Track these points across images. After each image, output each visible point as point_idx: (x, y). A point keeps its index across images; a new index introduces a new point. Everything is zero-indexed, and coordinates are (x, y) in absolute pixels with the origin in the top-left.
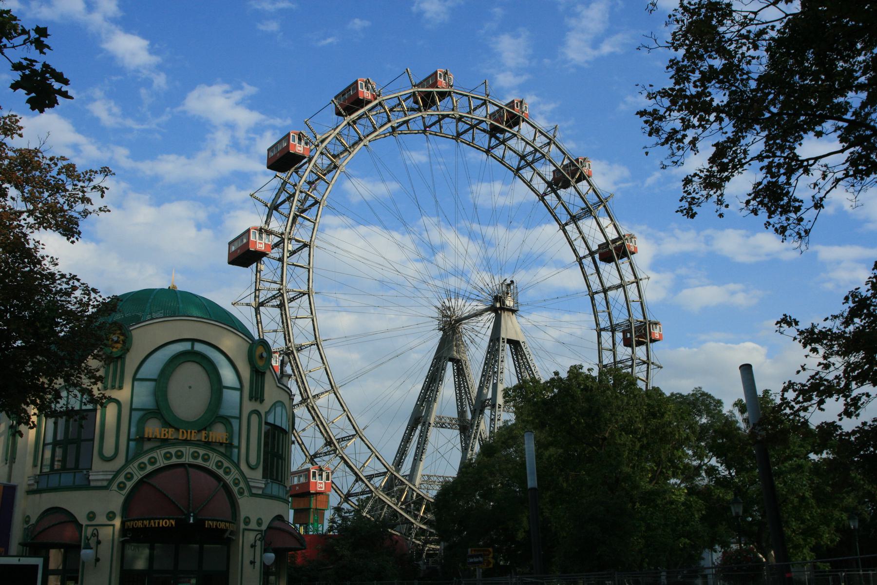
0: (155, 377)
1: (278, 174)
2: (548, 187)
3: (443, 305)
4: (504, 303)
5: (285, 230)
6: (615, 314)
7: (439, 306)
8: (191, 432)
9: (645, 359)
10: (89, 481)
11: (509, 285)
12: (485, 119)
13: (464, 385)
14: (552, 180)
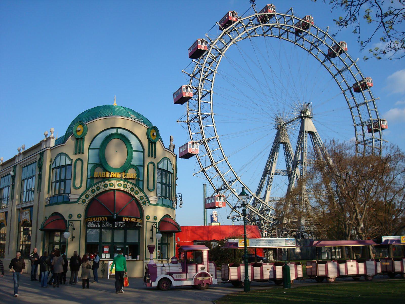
0: (98, 147)
1: (193, 60)
2: (326, 58)
4: (305, 113)
6: (363, 117)
8: (117, 174)
9: (379, 138)
10: (69, 199)
11: (307, 105)
12: (292, 26)
14: (328, 55)
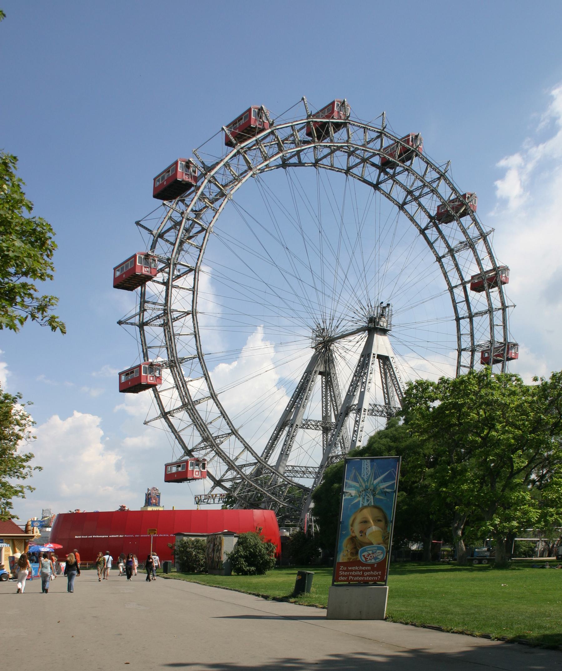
3: (317, 326)
5: (172, 256)
7: (315, 327)
13: (331, 394)
14: (436, 215)
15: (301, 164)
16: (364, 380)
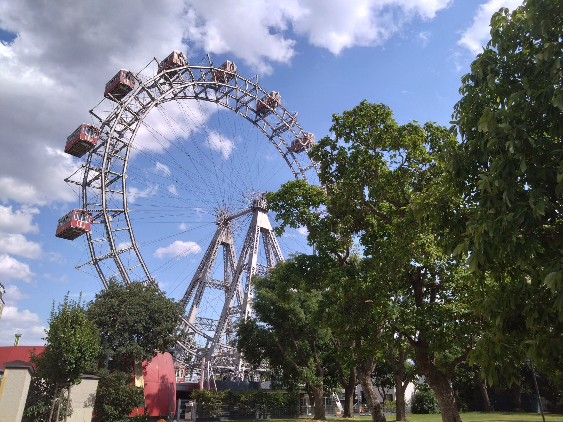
15: (185, 97)
16: (252, 245)
